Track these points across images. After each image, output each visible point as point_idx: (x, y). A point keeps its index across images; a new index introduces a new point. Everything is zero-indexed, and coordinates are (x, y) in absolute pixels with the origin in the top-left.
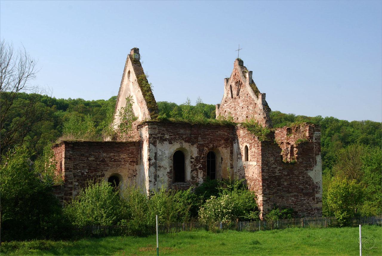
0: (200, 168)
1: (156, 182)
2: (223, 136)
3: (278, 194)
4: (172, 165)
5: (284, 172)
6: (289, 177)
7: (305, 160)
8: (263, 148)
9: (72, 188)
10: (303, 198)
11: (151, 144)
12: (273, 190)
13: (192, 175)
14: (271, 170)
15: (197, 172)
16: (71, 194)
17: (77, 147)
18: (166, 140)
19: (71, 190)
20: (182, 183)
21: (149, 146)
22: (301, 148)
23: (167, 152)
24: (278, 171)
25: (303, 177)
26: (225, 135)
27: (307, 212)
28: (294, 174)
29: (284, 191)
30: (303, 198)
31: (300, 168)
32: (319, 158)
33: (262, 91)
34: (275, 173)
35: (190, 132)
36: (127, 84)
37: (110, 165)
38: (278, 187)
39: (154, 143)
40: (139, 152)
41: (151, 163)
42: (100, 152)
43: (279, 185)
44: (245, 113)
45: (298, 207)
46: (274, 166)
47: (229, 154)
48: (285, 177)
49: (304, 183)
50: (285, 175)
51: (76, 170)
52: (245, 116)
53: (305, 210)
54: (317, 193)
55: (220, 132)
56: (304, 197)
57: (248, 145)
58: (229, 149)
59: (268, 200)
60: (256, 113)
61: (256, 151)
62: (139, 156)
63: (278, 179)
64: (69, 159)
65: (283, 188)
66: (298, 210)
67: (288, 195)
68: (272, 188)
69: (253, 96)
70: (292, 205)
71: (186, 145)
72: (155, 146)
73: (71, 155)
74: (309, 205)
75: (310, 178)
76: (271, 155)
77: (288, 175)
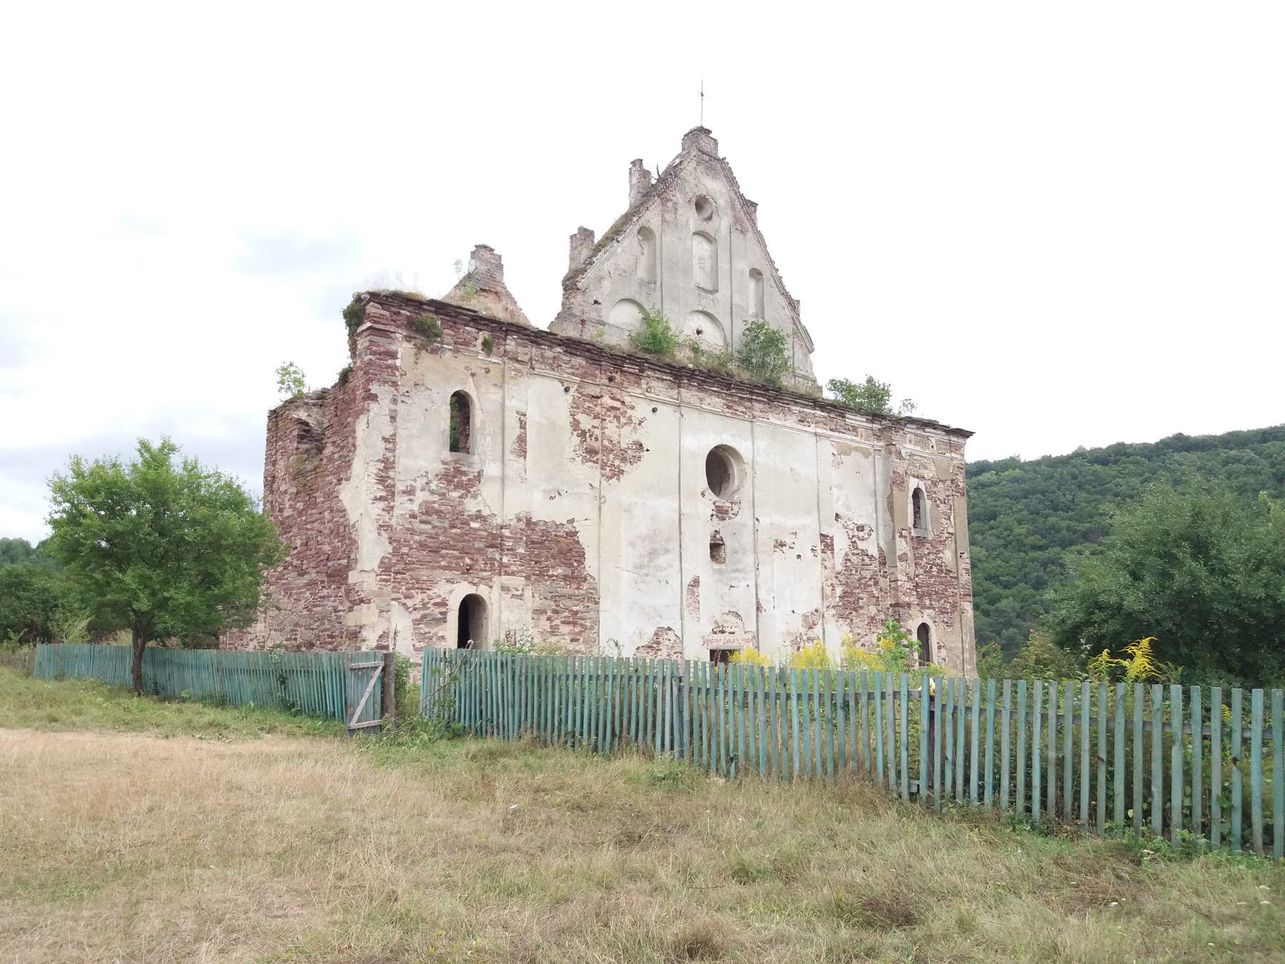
3: (283, 581)
5: (299, 502)
6: (304, 518)
10: (325, 592)
22: (333, 404)
27: (330, 646)
30: (325, 592)
46: (282, 489)
53: (329, 636)
54: (353, 569)
75: (343, 511)
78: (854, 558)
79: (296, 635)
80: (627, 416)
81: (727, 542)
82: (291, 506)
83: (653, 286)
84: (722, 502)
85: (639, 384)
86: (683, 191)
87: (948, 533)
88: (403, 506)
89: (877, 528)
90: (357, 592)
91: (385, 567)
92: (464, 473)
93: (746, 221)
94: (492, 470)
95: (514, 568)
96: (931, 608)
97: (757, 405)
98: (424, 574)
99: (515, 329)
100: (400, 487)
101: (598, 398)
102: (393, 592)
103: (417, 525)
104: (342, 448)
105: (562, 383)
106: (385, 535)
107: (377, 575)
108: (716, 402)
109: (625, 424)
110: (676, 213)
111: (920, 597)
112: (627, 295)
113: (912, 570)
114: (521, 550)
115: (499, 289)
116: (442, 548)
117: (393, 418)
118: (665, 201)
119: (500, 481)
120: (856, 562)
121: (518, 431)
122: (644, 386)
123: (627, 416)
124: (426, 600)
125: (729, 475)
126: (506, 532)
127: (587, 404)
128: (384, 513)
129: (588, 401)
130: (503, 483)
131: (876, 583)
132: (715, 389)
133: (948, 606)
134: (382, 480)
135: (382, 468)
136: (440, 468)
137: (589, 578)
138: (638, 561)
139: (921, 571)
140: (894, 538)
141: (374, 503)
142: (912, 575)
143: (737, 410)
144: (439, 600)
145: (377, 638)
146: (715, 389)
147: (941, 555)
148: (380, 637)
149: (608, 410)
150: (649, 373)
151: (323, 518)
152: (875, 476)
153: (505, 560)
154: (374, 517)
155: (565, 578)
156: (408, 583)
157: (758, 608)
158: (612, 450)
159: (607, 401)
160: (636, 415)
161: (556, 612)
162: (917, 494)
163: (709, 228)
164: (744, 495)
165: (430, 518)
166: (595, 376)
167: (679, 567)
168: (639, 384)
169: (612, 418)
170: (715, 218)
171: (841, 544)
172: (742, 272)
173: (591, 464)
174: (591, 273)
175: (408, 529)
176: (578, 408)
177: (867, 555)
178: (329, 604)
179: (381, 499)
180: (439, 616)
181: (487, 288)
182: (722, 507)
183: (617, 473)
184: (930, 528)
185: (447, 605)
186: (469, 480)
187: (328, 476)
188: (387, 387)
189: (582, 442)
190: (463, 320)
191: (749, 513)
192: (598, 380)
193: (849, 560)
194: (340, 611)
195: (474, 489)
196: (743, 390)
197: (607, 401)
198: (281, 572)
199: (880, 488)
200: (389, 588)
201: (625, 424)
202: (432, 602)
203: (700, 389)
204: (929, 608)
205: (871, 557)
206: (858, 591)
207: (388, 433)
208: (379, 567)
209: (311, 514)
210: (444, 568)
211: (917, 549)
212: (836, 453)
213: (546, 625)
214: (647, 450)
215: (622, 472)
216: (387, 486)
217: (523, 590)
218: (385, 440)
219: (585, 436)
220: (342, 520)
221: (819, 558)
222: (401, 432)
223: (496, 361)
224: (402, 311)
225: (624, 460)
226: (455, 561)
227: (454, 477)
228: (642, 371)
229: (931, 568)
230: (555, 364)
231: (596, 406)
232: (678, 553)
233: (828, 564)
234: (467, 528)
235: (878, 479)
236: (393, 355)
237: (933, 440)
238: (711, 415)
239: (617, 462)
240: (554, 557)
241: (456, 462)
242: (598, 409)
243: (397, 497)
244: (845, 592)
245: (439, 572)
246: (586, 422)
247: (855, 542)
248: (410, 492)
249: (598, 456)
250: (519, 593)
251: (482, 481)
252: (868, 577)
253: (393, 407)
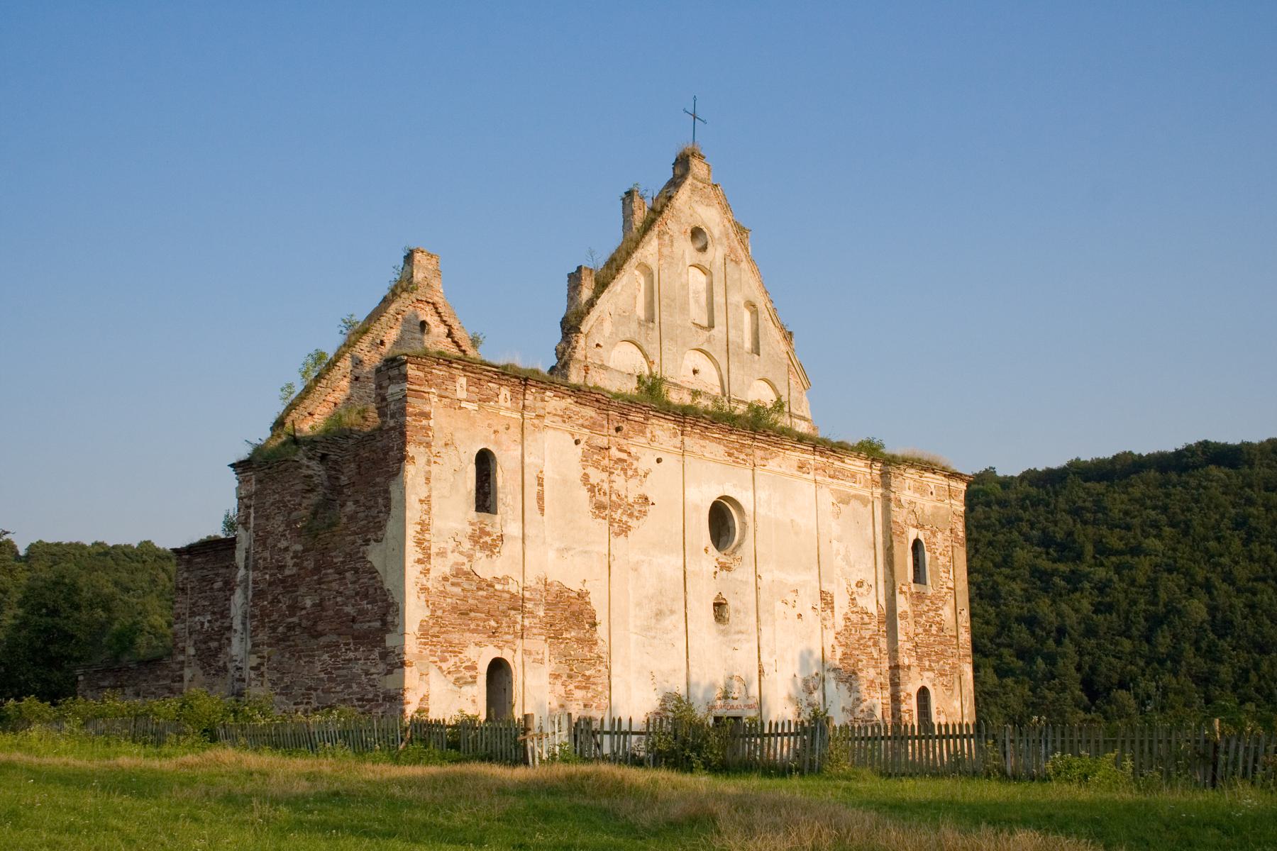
3: (288, 643)
5: (307, 560)
6: (315, 578)
7: (364, 505)
9: (183, 662)
10: (351, 655)
16: (181, 679)
19: (182, 669)
22: (354, 461)
24: (292, 558)
25: (356, 571)
28: (331, 565)
30: (351, 655)
31: (349, 538)
39: (246, 523)
41: (238, 580)
43: (293, 609)
45: (338, 689)
46: (283, 544)
49: (357, 594)
53: (358, 700)
56: (356, 650)
63: (289, 585)
67: (313, 643)
68: (275, 621)
70: (322, 680)
74: (370, 680)
75: (373, 572)
76: (279, 508)
77: (317, 570)
78: (853, 617)
79: (310, 698)
80: (633, 467)
81: (732, 603)
82: (295, 565)
83: (651, 325)
84: (723, 559)
85: (643, 432)
86: (679, 222)
87: (948, 588)
88: (440, 567)
89: (876, 583)
90: (399, 654)
91: (424, 632)
92: (488, 534)
93: (740, 251)
94: (513, 529)
95: (535, 631)
96: (931, 669)
97: (759, 453)
98: (455, 637)
99: (533, 383)
100: (434, 550)
101: (606, 449)
102: (431, 655)
103: (450, 589)
104: (369, 508)
105: (573, 435)
106: (423, 597)
107: (417, 638)
108: (718, 450)
109: (631, 477)
110: (672, 245)
111: (920, 658)
112: (628, 336)
113: (912, 627)
114: (542, 614)
115: (436, 299)
116: (471, 611)
117: (428, 479)
118: (660, 235)
119: (521, 541)
120: (855, 621)
121: (537, 488)
122: (649, 435)
123: (633, 467)
124: (459, 664)
125: (729, 527)
126: (527, 594)
127: (596, 456)
128: (422, 576)
129: (596, 453)
130: (523, 542)
131: (875, 644)
132: (716, 436)
133: (947, 668)
134: (419, 543)
135: (419, 530)
136: (469, 530)
137: (599, 641)
138: (646, 624)
139: (920, 630)
140: (894, 594)
141: (412, 566)
142: (912, 635)
143: (737, 458)
144: (469, 664)
145: (419, 701)
146: (716, 436)
147: (940, 612)
148: (421, 700)
149: (616, 463)
150: (654, 421)
151: (344, 578)
152: (874, 526)
153: (527, 622)
154: (414, 580)
155: (579, 640)
156: (442, 646)
157: (761, 672)
158: (620, 505)
159: (614, 452)
160: (642, 466)
161: (570, 677)
162: (917, 545)
163: (705, 259)
164: (747, 549)
165: (460, 581)
166: (603, 426)
167: (684, 629)
168: (643, 432)
169: (618, 472)
170: (710, 248)
171: (841, 604)
172: (738, 306)
173: (600, 520)
174: (594, 314)
175: (441, 592)
176: (587, 461)
177: (867, 613)
178: (357, 668)
179: (419, 561)
180: (470, 680)
181: (424, 299)
182: (725, 563)
183: (625, 530)
184: (929, 582)
185: (476, 669)
186: (493, 540)
187: (350, 535)
188: (422, 449)
189: (591, 497)
190: (485, 375)
191: (752, 569)
192: (606, 430)
193: (849, 619)
194: (372, 674)
195: (498, 549)
196: (744, 436)
197: (614, 452)
198: (284, 633)
199: (880, 539)
200: (428, 652)
201: (631, 477)
202: (464, 665)
203: (703, 437)
204: (928, 670)
205: (870, 615)
206: (857, 653)
207: (423, 496)
208: (419, 630)
209: (326, 574)
210: (473, 631)
211: (917, 605)
212: (835, 502)
213: (560, 690)
214: (653, 504)
215: (629, 528)
216: (424, 549)
217: (543, 653)
218: (421, 501)
219: (594, 492)
220: (371, 581)
221: (819, 618)
222: (434, 494)
223: (515, 416)
224: (433, 371)
225: (631, 515)
226: (482, 624)
227: (481, 537)
228: (647, 419)
229: (931, 626)
230: (566, 417)
231: (604, 458)
232: (683, 614)
233: (828, 624)
234: (491, 590)
235: (877, 529)
236: (427, 416)
237: (932, 486)
238: (712, 464)
239: (625, 518)
240: (566, 619)
241: (481, 523)
242: (606, 462)
243: (432, 561)
244: (844, 654)
245: (468, 635)
246: (596, 476)
247: (854, 599)
248: (442, 554)
249: (607, 512)
250: (539, 657)
251: (505, 541)
252: (867, 637)
253: (427, 468)
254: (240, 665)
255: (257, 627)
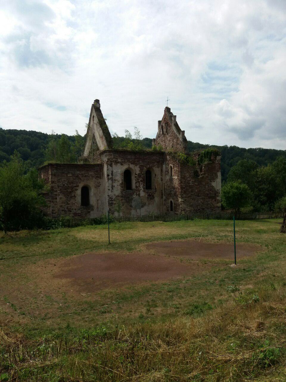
0: (141, 181)
1: (113, 190)
2: (156, 160)
4: (123, 179)
8: (181, 167)
11: (109, 166)
12: (187, 195)
13: (136, 185)
14: (187, 182)
15: (139, 184)
16: (56, 198)
17: (59, 168)
18: (119, 163)
20: (130, 190)
21: (108, 167)
23: (119, 171)
25: (209, 186)
26: (157, 159)
29: (195, 195)
31: (206, 180)
32: (219, 174)
33: (182, 130)
34: (190, 183)
35: (134, 157)
36: (92, 125)
37: (82, 179)
38: (192, 192)
40: (102, 170)
42: (75, 171)
43: (192, 192)
44: (171, 144)
46: (189, 179)
47: (160, 172)
48: (196, 186)
50: (196, 185)
51: (59, 183)
52: (171, 146)
55: (154, 157)
57: (172, 166)
58: (160, 168)
59: (185, 201)
60: (178, 144)
61: (177, 169)
62: (102, 173)
64: (54, 175)
65: (194, 193)
66: (205, 208)
67: (198, 198)
69: (177, 134)
71: (132, 166)
72: (112, 167)
73: (56, 173)
254: (112, 197)
255: (183, 194)
